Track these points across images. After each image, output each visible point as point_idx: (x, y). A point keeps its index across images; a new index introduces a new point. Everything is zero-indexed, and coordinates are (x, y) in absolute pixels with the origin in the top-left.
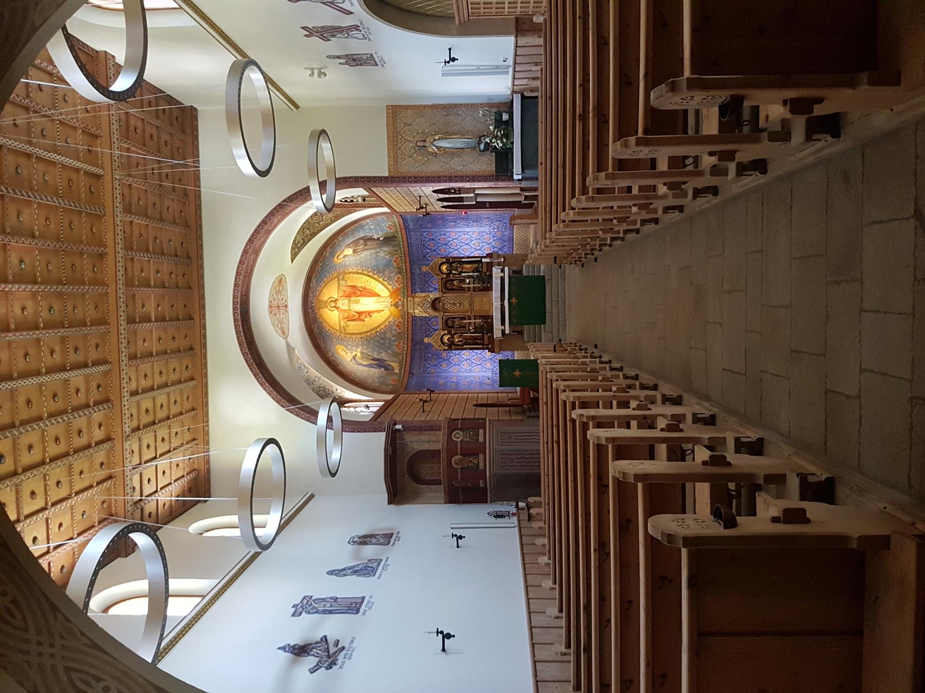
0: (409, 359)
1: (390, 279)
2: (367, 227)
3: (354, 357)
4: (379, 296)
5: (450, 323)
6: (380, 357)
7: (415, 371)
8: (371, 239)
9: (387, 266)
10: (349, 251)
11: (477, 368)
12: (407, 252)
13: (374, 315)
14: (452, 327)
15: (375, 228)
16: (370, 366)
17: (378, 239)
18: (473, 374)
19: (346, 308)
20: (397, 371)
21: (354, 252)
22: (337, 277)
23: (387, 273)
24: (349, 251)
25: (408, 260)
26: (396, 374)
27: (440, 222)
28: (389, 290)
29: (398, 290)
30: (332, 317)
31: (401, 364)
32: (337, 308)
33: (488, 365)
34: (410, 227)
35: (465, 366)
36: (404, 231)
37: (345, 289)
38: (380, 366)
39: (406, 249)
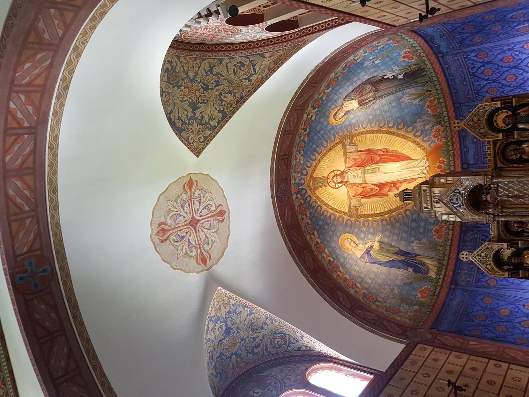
1: (424, 133)
2: (367, 64)
3: (368, 252)
4: (409, 159)
6: (409, 249)
9: (418, 114)
10: (354, 105)
12: (446, 91)
15: (384, 63)
16: (391, 264)
19: (359, 180)
20: (432, 274)
21: (360, 103)
22: (341, 142)
23: (419, 126)
25: (449, 102)
26: (429, 280)
27: (497, 27)
28: (424, 149)
29: (437, 148)
30: (335, 197)
31: (440, 263)
32: (346, 183)
34: (443, 49)
36: (433, 58)
37: (354, 156)
39: (444, 85)
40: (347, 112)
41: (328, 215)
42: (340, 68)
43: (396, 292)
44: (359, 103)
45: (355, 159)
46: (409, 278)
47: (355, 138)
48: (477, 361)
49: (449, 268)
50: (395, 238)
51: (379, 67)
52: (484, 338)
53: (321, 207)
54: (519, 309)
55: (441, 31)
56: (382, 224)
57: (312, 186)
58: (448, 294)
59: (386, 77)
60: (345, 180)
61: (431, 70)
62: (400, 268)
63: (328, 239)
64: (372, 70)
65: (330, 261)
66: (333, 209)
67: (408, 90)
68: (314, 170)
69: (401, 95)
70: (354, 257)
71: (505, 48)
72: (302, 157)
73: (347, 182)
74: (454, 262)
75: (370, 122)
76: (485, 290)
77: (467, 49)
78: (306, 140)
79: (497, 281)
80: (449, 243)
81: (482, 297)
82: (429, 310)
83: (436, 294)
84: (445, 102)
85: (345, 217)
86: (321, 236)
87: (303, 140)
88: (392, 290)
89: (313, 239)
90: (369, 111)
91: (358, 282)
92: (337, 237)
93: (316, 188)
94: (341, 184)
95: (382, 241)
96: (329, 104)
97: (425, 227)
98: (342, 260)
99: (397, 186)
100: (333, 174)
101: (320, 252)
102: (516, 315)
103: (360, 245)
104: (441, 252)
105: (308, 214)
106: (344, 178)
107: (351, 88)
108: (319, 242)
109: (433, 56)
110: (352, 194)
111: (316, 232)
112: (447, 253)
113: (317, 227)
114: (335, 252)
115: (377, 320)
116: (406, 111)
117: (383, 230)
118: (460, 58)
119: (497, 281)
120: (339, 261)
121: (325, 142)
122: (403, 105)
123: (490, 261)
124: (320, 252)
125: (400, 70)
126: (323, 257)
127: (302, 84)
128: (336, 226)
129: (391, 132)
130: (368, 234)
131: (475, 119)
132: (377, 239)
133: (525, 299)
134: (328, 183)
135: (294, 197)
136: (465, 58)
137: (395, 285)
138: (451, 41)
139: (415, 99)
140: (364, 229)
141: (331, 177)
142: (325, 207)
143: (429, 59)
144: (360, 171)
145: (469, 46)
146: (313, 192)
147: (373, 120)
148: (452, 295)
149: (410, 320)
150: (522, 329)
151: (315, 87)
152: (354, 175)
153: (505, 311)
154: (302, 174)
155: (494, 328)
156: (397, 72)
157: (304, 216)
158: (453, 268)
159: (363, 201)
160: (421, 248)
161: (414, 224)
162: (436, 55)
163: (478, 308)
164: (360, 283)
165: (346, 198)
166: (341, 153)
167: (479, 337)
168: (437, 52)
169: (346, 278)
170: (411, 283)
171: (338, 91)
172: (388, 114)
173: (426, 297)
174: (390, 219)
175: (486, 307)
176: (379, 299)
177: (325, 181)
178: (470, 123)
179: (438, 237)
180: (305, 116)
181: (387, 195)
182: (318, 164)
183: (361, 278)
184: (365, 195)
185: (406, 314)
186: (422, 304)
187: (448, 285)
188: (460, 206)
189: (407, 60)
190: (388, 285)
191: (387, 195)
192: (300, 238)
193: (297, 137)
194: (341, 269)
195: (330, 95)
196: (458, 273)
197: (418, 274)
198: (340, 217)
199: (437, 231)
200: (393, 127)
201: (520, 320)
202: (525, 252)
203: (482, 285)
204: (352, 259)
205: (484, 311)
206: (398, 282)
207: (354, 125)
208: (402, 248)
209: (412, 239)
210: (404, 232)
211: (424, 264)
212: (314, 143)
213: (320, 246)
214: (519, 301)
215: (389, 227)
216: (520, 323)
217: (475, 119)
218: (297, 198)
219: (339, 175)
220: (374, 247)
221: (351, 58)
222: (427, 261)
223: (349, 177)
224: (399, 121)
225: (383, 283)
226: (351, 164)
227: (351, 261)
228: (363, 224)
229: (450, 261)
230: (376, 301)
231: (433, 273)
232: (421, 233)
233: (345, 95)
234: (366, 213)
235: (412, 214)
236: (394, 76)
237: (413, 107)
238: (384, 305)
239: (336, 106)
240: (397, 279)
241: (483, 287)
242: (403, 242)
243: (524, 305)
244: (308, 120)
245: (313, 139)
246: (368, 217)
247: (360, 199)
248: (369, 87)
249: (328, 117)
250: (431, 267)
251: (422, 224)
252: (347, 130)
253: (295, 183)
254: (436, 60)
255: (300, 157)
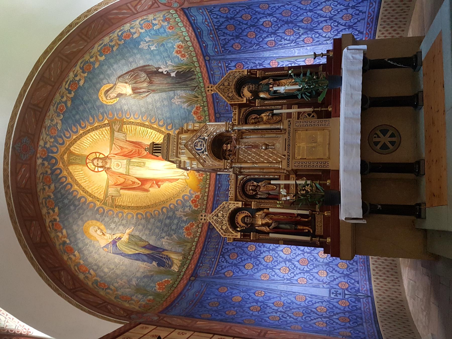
0: (199, 250)
3: (114, 242)
5: (249, 187)
6: (158, 244)
7: (202, 272)
8: (157, 73)
11: (302, 279)
13: (165, 186)
14: (253, 197)
16: (137, 257)
17: (168, 74)
18: (295, 289)
20: (175, 268)
21: (134, 89)
24: (126, 89)
26: (172, 273)
27: (251, 35)
30: (91, 180)
31: (185, 257)
32: (107, 170)
33: (323, 275)
34: (210, 51)
35: (282, 271)
37: (122, 144)
38: (151, 258)
40: (119, 95)
41: (78, 197)
42: (115, 34)
43: (134, 282)
44: (133, 90)
45: (122, 148)
46: (150, 271)
47: (125, 126)
48: (201, 336)
49: (192, 261)
50: (147, 232)
51: (154, 55)
52: (215, 320)
53: (71, 185)
54: (250, 296)
55: (208, 25)
56: (137, 218)
57: (66, 159)
58: (187, 284)
59: (160, 70)
60: (108, 166)
61: (199, 75)
62: (145, 261)
63: (71, 220)
64: (148, 56)
65: (64, 242)
66: (86, 192)
67: (179, 92)
68: (72, 144)
69: (173, 95)
70: (97, 245)
71: (257, 62)
72: (60, 122)
73: (109, 168)
74: (198, 256)
75: (143, 114)
76: (222, 281)
77: (228, 57)
78: (69, 104)
79: (234, 273)
80: (196, 239)
81: (218, 286)
82: (164, 299)
83: (175, 286)
84: (208, 111)
85: (98, 203)
86: (62, 215)
87: (65, 103)
88: (129, 281)
89: (51, 215)
90: (142, 102)
91: (93, 269)
92: (82, 221)
93: (71, 164)
94: (102, 169)
95: (132, 234)
96: (102, 76)
97: (178, 224)
98: (80, 245)
99: (159, 183)
100: (94, 156)
101: (56, 230)
102: (246, 302)
103: (108, 235)
104: (188, 248)
105: (52, 186)
106: (106, 163)
107: (126, 69)
108: (58, 220)
109: (202, 57)
110: (111, 183)
111: (56, 209)
112: (193, 248)
113: (60, 205)
114: (75, 236)
115: (100, 304)
116: (176, 113)
117: (136, 223)
118: (223, 65)
119: (234, 273)
120: (77, 245)
121: (91, 118)
122: (174, 106)
123: (226, 221)
124: (56, 230)
125: (174, 66)
126: (58, 236)
127: (70, 26)
128: (85, 210)
129: (160, 130)
130: (120, 225)
131: (226, 84)
132: (128, 231)
133: (257, 288)
134: (87, 164)
135: (39, 161)
136: (227, 67)
137: (133, 277)
138: (217, 43)
139: (184, 102)
140: (116, 219)
141: (91, 157)
142: (76, 187)
143: (198, 61)
144: (125, 161)
145: (230, 53)
146: (66, 165)
147: (145, 113)
148: (190, 286)
149: (139, 307)
150: (251, 312)
151: (86, 41)
152: (117, 164)
153: (237, 298)
154: (56, 141)
155: (225, 312)
156: (170, 68)
157: (47, 188)
158: (196, 262)
159: (122, 192)
160: (169, 243)
161: (168, 221)
162: (204, 57)
163: (213, 297)
164: (95, 271)
165: (104, 184)
166: (108, 137)
167: (208, 319)
168: (205, 55)
169: (80, 263)
170: (152, 276)
171: (112, 66)
172: (159, 112)
173: (164, 288)
174: (146, 214)
175: (220, 296)
176: (112, 287)
177: (83, 160)
178: (221, 87)
179: (187, 234)
180: (71, 75)
181: (147, 191)
182: (78, 138)
183: (98, 266)
184: (125, 186)
185: (138, 301)
186: (158, 295)
187: (188, 277)
188: (203, 152)
189: (180, 57)
190: (127, 276)
191: (147, 191)
192: (32, 207)
193: (58, 95)
194: (76, 253)
195: (103, 65)
196: (200, 267)
197: (162, 268)
198: (92, 202)
199: (187, 229)
200: (162, 126)
201: (250, 305)
202: (258, 213)
203: (219, 277)
204: (94, 246)
205: (218, 299)
206: (139, 275)
207: (126, 112)
208: (151, 243)
209: (164, 235)
210: (157, 227)
211: (169, 258)
212: (77, 113)
213: (56, 224)
214: (250, 290)
215: (143, 221)
216: (249, 308)
217: (226, 84)
218: (43, 164)
219: (101, 159)
220: (122, 239)
221: (127, 27)
222: (173, 256)
223: (112, 164)
224: (169, 121)
225: (122, 274)
226: (116, 152)
227: (91, 249)
228: (117, 214)
229: (195, 255)
230: (106, 289)
231: (176, 267)
232: (173, 230)
233: (119, 74)
234: (122, 204)
235: (168, 212)
236: (168, 72)
237: (182, 111)
238: (116, 292)
239: (109, 83)
240: (138, 271)
241: (220, 278)
242: (153, 237)
243: (254, 293)
244: (74, 83)
245: (78, 109)
246: (124, 209)
247: (119, 189)
248: (143, 75)
249: (98, 90)
250: (175, 261)
251: (176, 221)
252: (117, 115)
253: (45, 147)
254: (203, 64)
255: (58, 121)
